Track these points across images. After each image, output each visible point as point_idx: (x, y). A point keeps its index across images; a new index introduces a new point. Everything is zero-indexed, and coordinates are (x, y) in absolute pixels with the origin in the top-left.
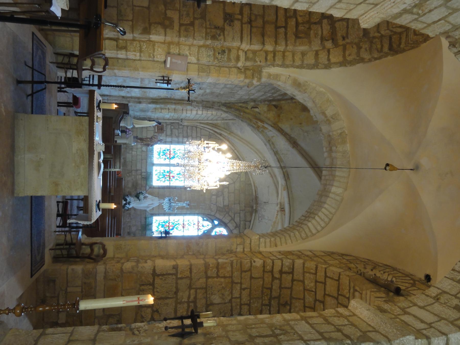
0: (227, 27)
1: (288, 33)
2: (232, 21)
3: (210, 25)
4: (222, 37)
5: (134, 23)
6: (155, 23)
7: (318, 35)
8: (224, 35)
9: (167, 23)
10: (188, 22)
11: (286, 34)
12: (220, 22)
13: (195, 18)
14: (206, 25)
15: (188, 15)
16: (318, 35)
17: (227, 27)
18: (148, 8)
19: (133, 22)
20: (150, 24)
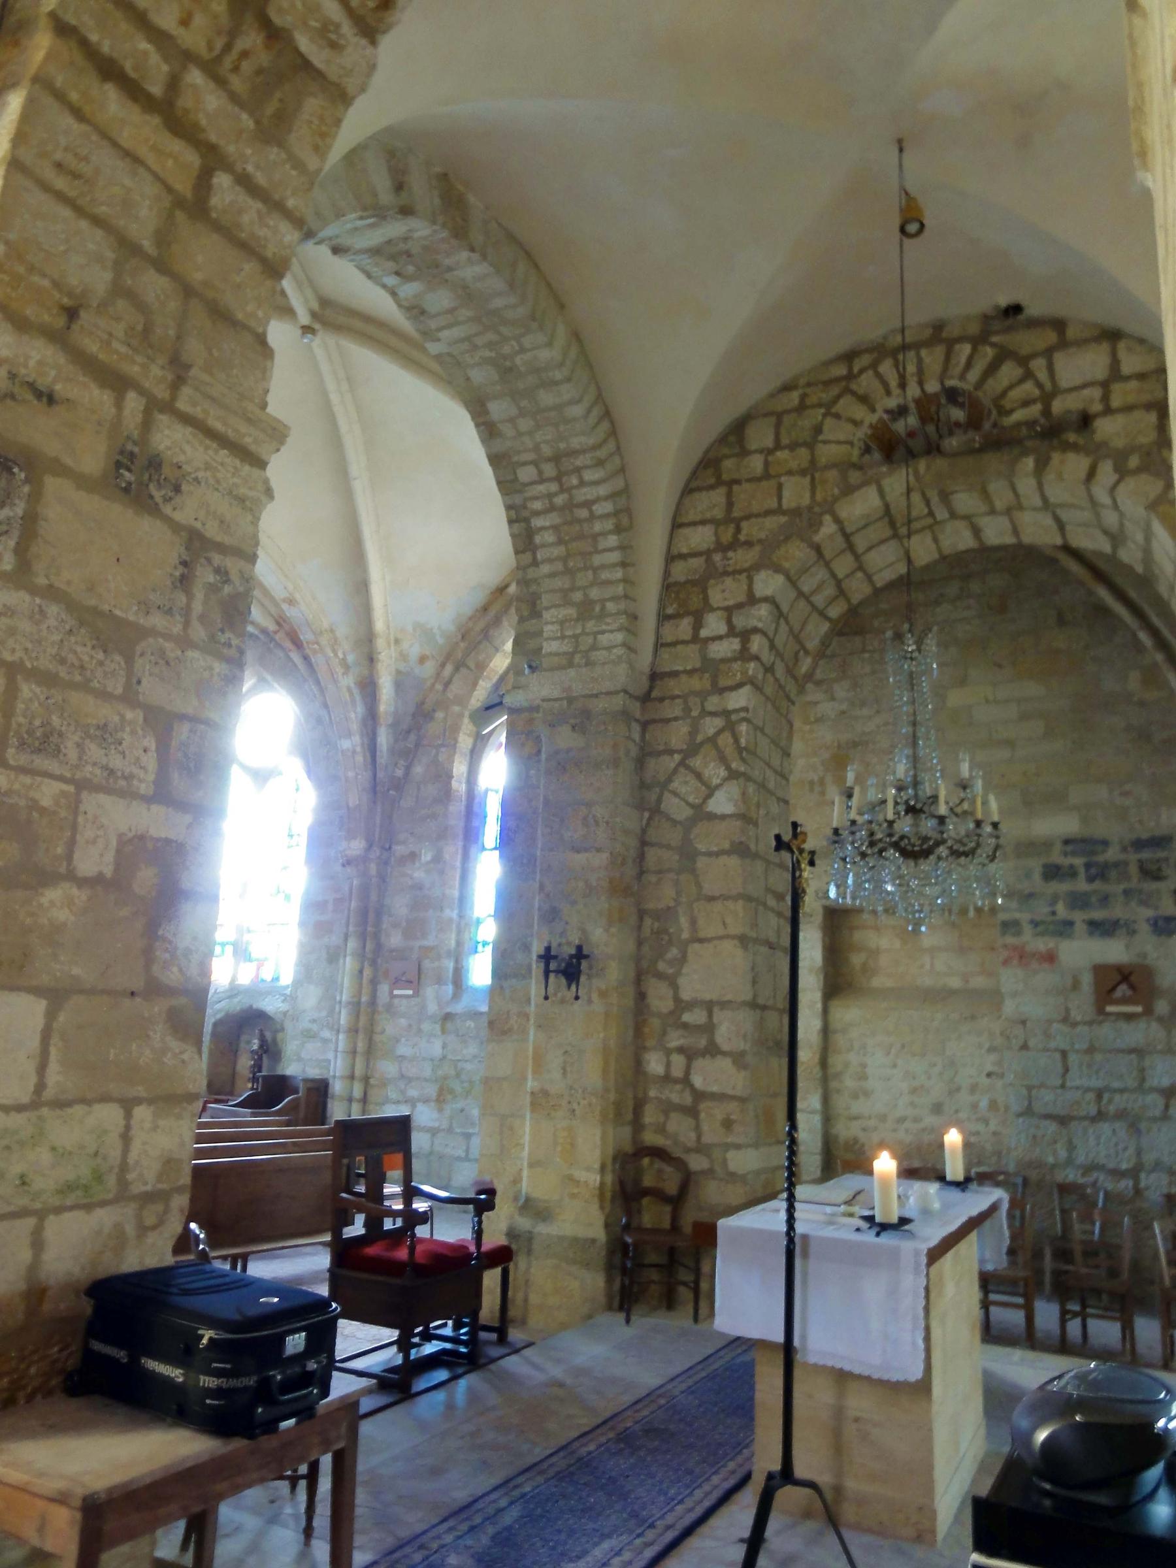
0: (186, 511)
1: (250, 168)
2: (155, 463)
3: (169, 612)
4: (233, 565)
5: (140, 1091)
6: (148, 955)
7: (338, 26)
8: (222, 549)
9: (145, 878)
10: (150, 742)
11: (244, 181)
12: (152, 543)
13: (129, 698)
14: (168, 637)
15: (105, 734)
16: (338, 26)
17: (186, 511)
18: (56, 996)
19: (138, 1101)
20: (154, 989)
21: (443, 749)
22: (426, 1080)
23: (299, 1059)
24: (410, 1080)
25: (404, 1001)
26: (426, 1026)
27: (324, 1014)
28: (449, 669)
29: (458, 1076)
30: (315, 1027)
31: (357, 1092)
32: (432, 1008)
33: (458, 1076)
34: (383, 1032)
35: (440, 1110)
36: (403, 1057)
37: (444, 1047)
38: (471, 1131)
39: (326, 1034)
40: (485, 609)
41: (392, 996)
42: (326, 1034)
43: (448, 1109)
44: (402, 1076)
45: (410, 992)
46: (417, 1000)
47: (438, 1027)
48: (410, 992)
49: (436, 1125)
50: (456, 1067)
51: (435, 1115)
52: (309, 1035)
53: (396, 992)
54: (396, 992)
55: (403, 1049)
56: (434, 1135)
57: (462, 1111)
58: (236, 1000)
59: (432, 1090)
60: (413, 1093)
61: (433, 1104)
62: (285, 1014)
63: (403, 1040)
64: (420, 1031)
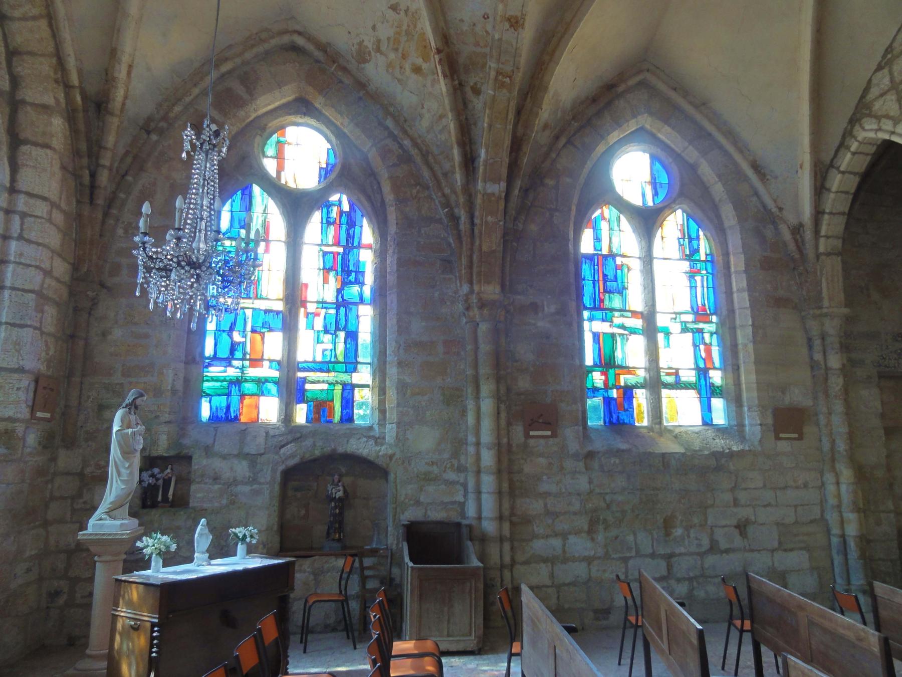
21: (557, 214)
22: (575, 514)
23: (418, 503)
24: (556, 515)
25: (542, 441)
26: (569, 464)
27: (446, 456)
28: (563, 141)
29: (608, 507)
30: (435, 469)
31: (506, 531)
32: (573, 446)
33: (608, 507)
34: (520, 471)
35: (593, 539)
36: (547, 494)
37: (590, 482)
38: (628, 555)
39: (451, 476)
40: (594, 100)
41: (527, 436)
42: (451, 476)
43: (600, 537)
44: (548, 513)
45: (549, 433)
46: (556, 440)
47: (581, 465)
48: (549, 433)
49: (592, 553)
50: (604, 499)
51: (589, 544)
52: (427, 478)
53: (532, 433)
54: (532, 433)
55: (544, 487)
56: (589, 564)
57: (616, 538)
58: (308, 442)
59: (583, 522)
60: (562, 525)
61: (584, 535)
62: (391, 457)
63: (545, 478)
64: (562, 468)
